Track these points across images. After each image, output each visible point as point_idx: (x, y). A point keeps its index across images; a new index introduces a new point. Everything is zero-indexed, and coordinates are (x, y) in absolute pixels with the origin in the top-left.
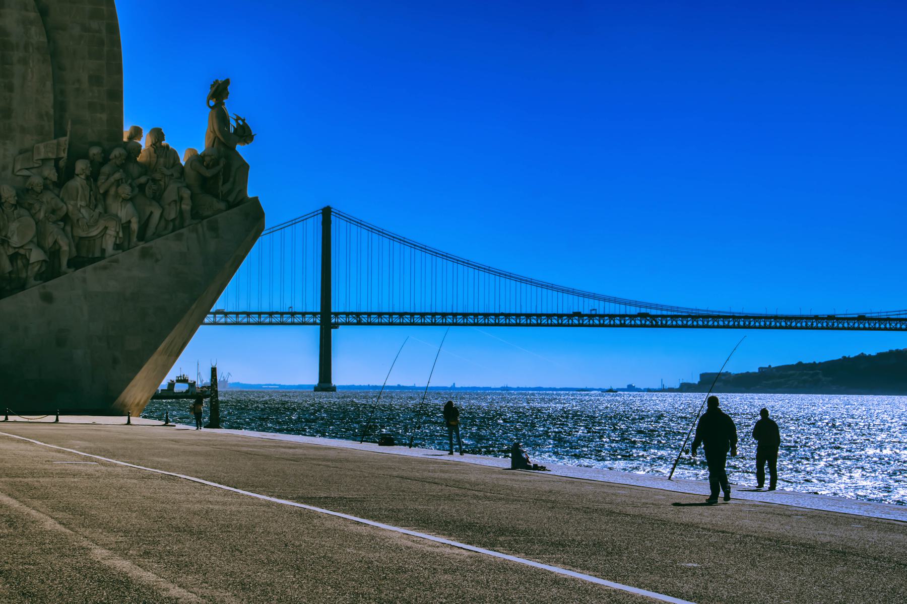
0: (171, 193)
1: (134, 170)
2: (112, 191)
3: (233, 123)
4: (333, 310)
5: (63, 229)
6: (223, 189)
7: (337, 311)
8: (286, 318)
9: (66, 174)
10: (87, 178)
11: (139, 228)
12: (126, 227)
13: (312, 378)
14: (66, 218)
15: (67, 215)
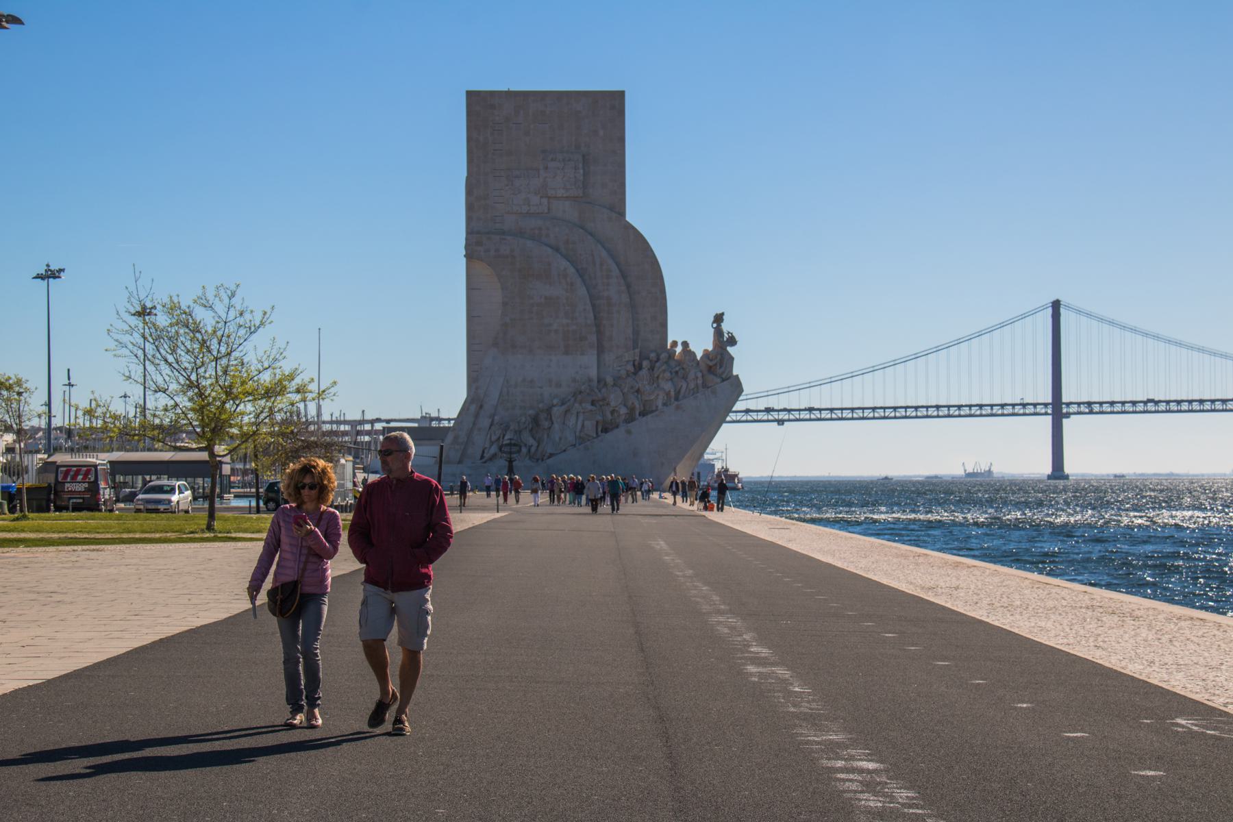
0: (691, 376)
1: (673, 363)
2: (661, 376)
3: (726, 335)
4: (1064, 400)
5: (637, 397)
6: (719, 371)
7: (1068, 401)
8: (1018, 409)
9: (638, 368)
10: (649, 369)
11: (675, 394)
12: (668, 394)
13: (1044, 468)
14: (638, 391)
15: (639, 389)
